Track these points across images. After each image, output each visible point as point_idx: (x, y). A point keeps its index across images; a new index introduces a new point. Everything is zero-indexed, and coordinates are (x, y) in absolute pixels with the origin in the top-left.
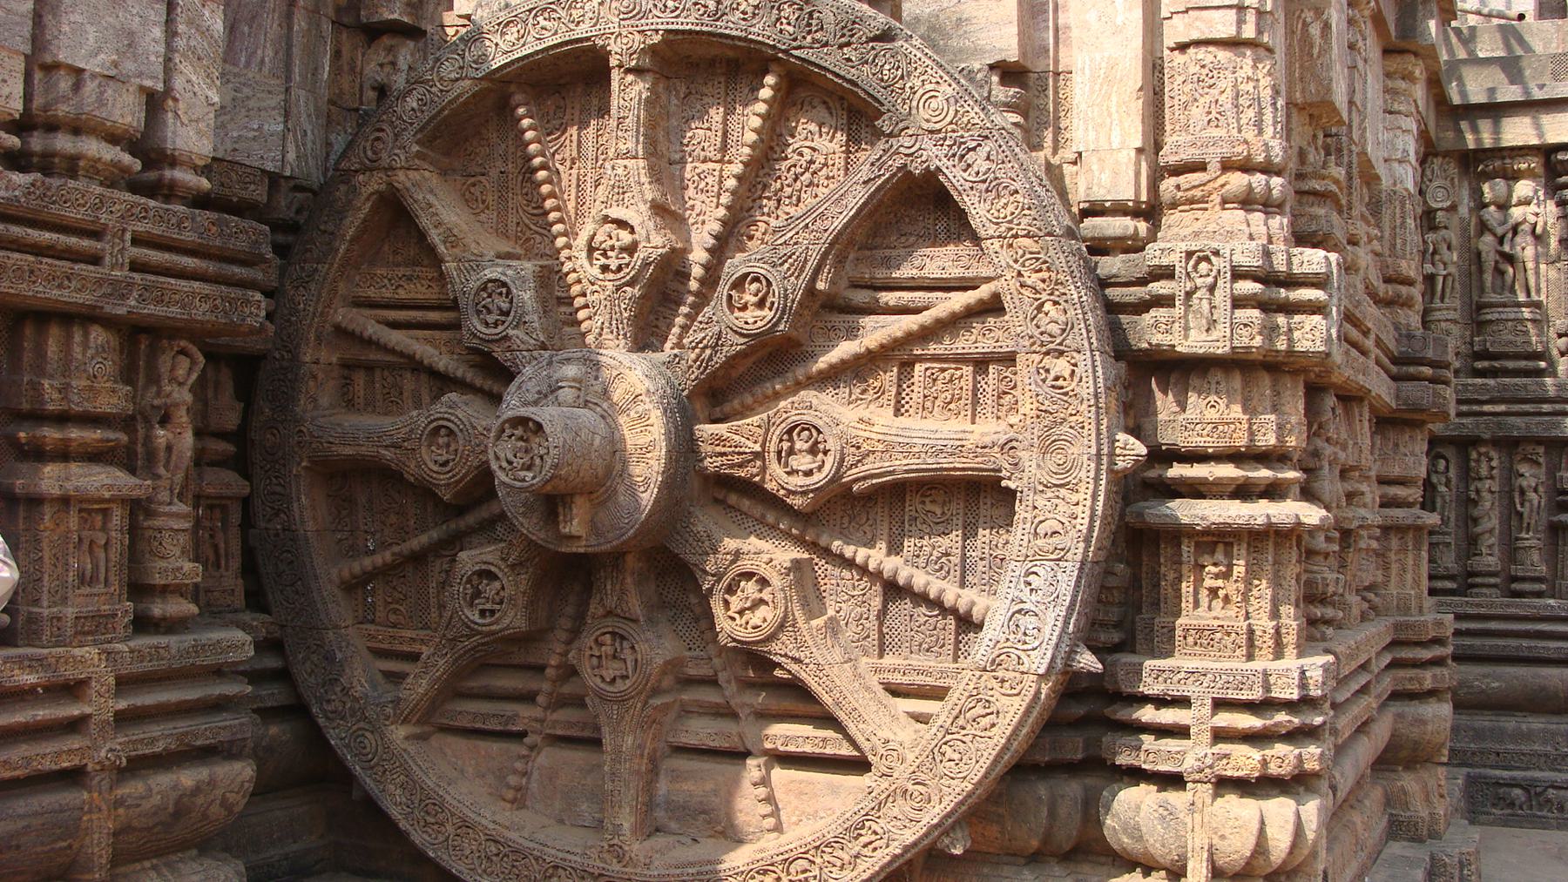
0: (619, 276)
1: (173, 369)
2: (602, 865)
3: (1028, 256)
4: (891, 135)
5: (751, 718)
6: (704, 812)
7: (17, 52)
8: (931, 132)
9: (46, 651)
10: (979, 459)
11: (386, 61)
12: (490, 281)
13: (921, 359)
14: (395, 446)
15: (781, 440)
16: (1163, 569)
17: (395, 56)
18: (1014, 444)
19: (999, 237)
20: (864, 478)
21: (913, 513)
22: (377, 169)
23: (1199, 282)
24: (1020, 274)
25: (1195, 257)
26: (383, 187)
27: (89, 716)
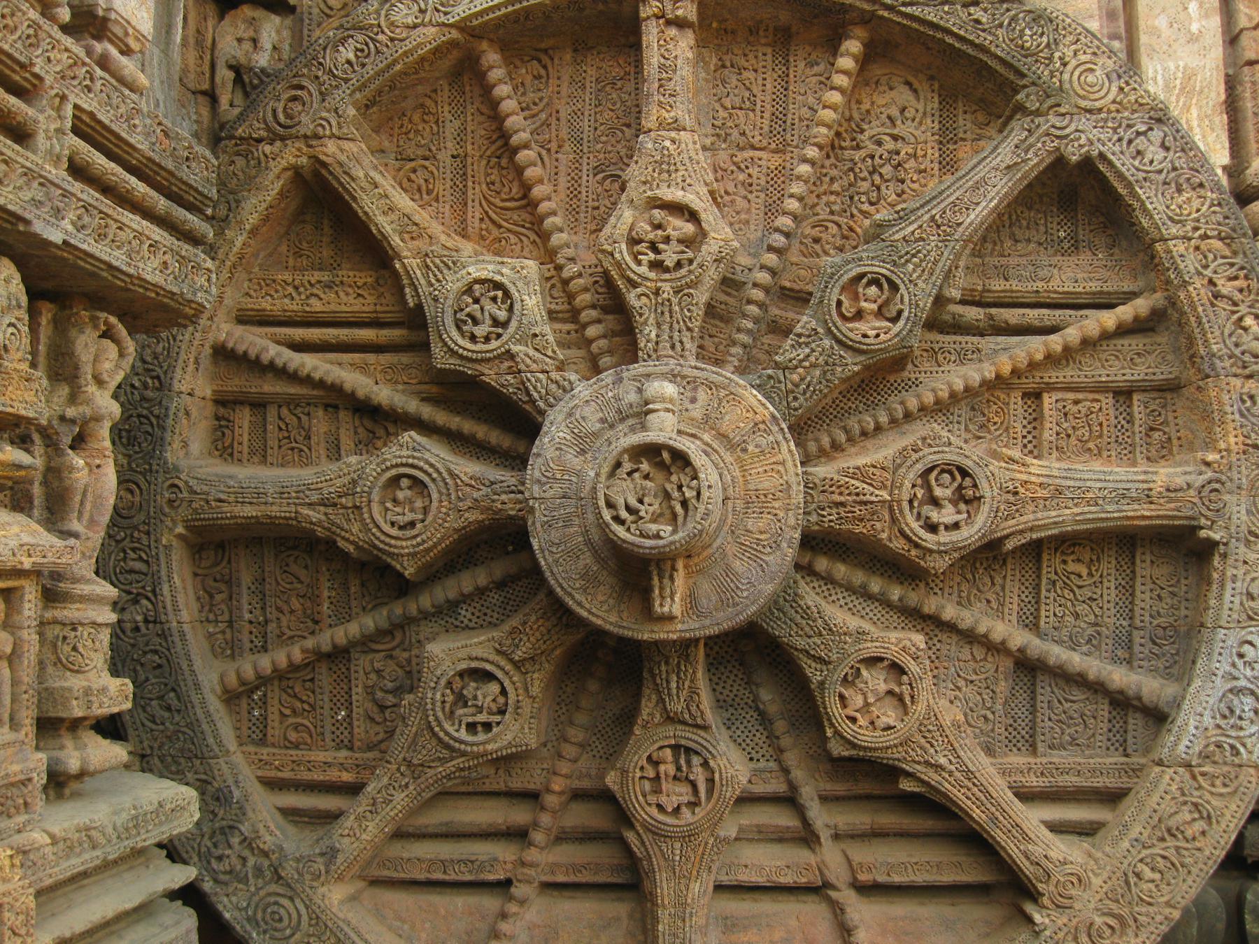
4: (1037, 113)
5: (830, 842)
8: (1090, 111)
10: (1172, 505)
11: (246, 35)
12: (477, 281)
13: (1051, 388)
15: (914, 486)
18: (1217, 486)
19: (1184, 237)
20: (1022, 532)
24: (1211, 282)
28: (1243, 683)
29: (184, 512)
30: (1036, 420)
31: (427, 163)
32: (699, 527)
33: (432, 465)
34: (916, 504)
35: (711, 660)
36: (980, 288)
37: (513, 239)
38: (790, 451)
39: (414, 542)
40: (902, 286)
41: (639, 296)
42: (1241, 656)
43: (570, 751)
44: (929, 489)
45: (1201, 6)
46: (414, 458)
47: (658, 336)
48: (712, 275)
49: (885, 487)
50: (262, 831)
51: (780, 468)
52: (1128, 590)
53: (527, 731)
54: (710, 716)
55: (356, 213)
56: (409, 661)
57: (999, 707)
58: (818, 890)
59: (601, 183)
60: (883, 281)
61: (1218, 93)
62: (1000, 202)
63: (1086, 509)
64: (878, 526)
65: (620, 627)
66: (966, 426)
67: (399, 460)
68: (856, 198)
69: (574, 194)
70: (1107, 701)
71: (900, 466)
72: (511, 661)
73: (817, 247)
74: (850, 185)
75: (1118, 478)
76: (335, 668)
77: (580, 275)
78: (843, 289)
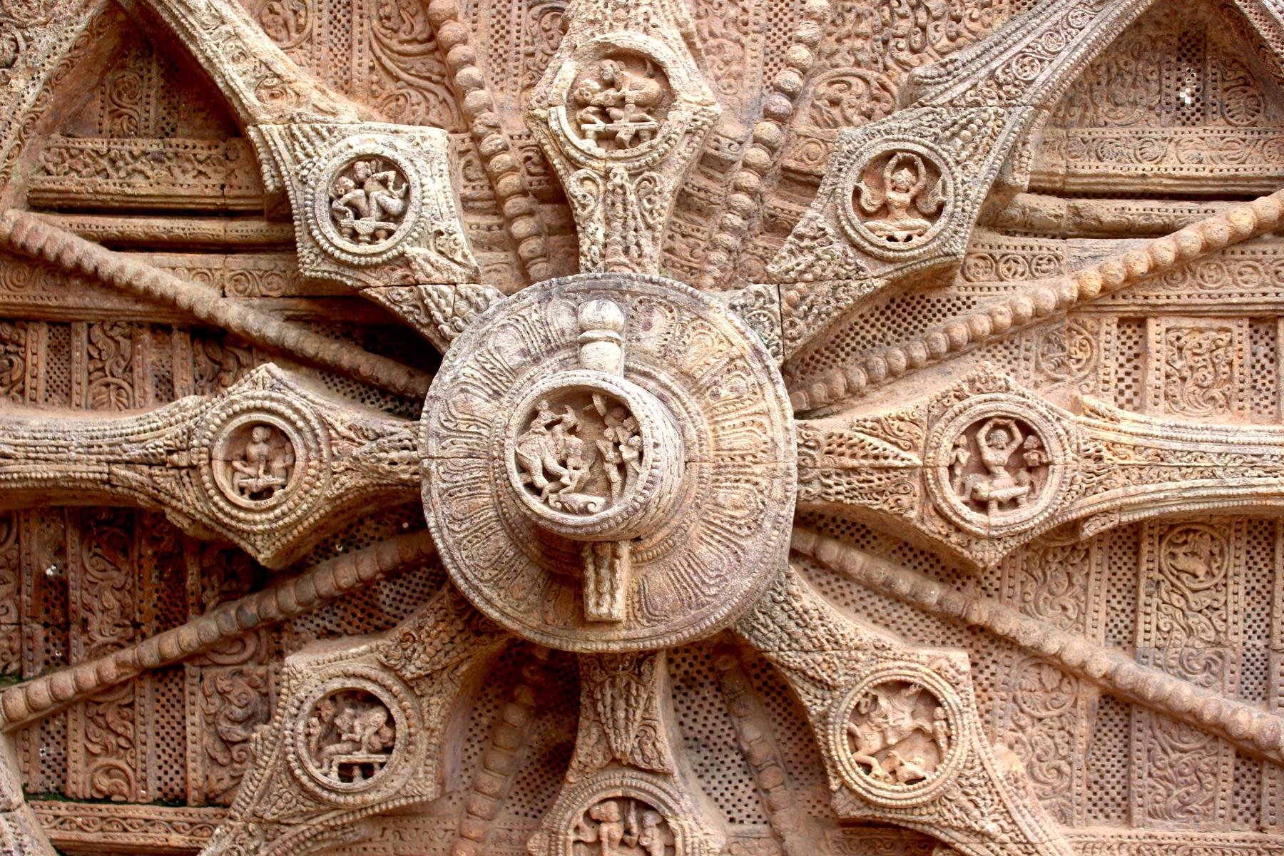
0: (630, 152)
12: (360, 157)
13: (1159, 311)
15: (956, 447)
20: (1106, 512)
21: (1156, 575)
30: (1139, 356)
32: (641, 499)
33: (297, 411)
34: (958, 471)
35: (677, 682)
36: (1061, 171)
37: (415, 97)
38: (778, 397)
39: (271, 515)
40: (944, 170)
41: (583, 180)
43: (481, 804)
44: (978, 451)
46: (272, 399)
47: (606, 236)
48: (683, 152)
49: (913, 447)
51: (764, 420)
53: (421, 775)
54: (669, 757)
55: (195, 59)
56: (265, 679)
57: (1078, 756)
59: (537, 19)
60: (919, 162)
62: (1090, 50)
63: (1199, 482)
64: (905, 500)
65: (543, 633)
66: (1037, 363)
67: (251, 403)
68: (892, 43)
69: (500, 34)
70: (1231, 752)
71: (938, 418)
72: (401, 679)
73: (835, 112)
74: (884, 25)
75: (1246, 440)
76: (163, 689)
77: (506, 149)
78: (863, 173)
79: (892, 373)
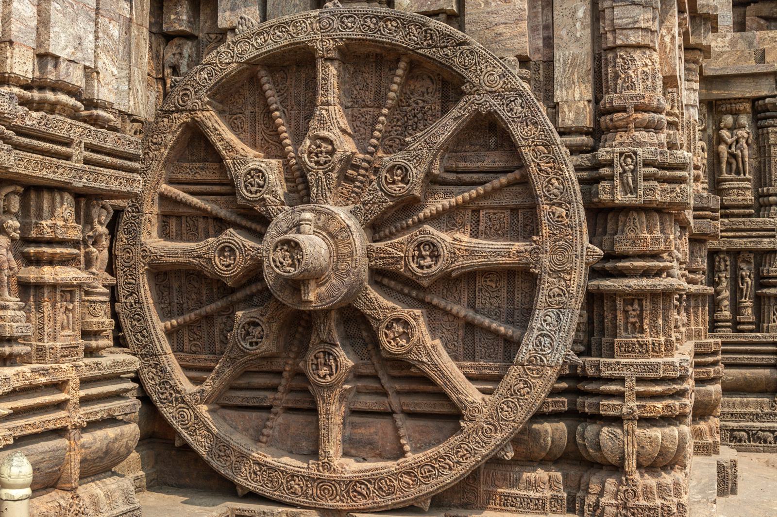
0: (323, 167)
1: (99, 216)
2: (318, 473)
3: (542, 155)
4: (470, 94)
5: (395, 394)
6: (370, 444)
7: (30, 47)
8: (491, 92)
9: (49, 366)
11: (177, 52)
12: (252, 169)
13: (483, 208)
14: (200, 257)
15: (414, 250)
16: (606, 313)
17: (181, 50)
18: (537, 250)
20: (458, 269)
21: (481, 287)
22: (186, 110)
23: (627, 168)
24: (538, 164)
25: (624, 156)
26: (189, 119)
27: (68, 400)
28: (545, 332)
29: (148, 260)
31: (241, 116)
33: (237, 242)
37: (274, 148)
40: (410, 170)
42: (545, 321)
45: (582, 24)
49: (402, 251)
50: (178, 383)
52: (511, 293)
58: (388, 414)
61: (589, 64)
64: (399, 266)
73: (391, 149)
79: (403, 228)
